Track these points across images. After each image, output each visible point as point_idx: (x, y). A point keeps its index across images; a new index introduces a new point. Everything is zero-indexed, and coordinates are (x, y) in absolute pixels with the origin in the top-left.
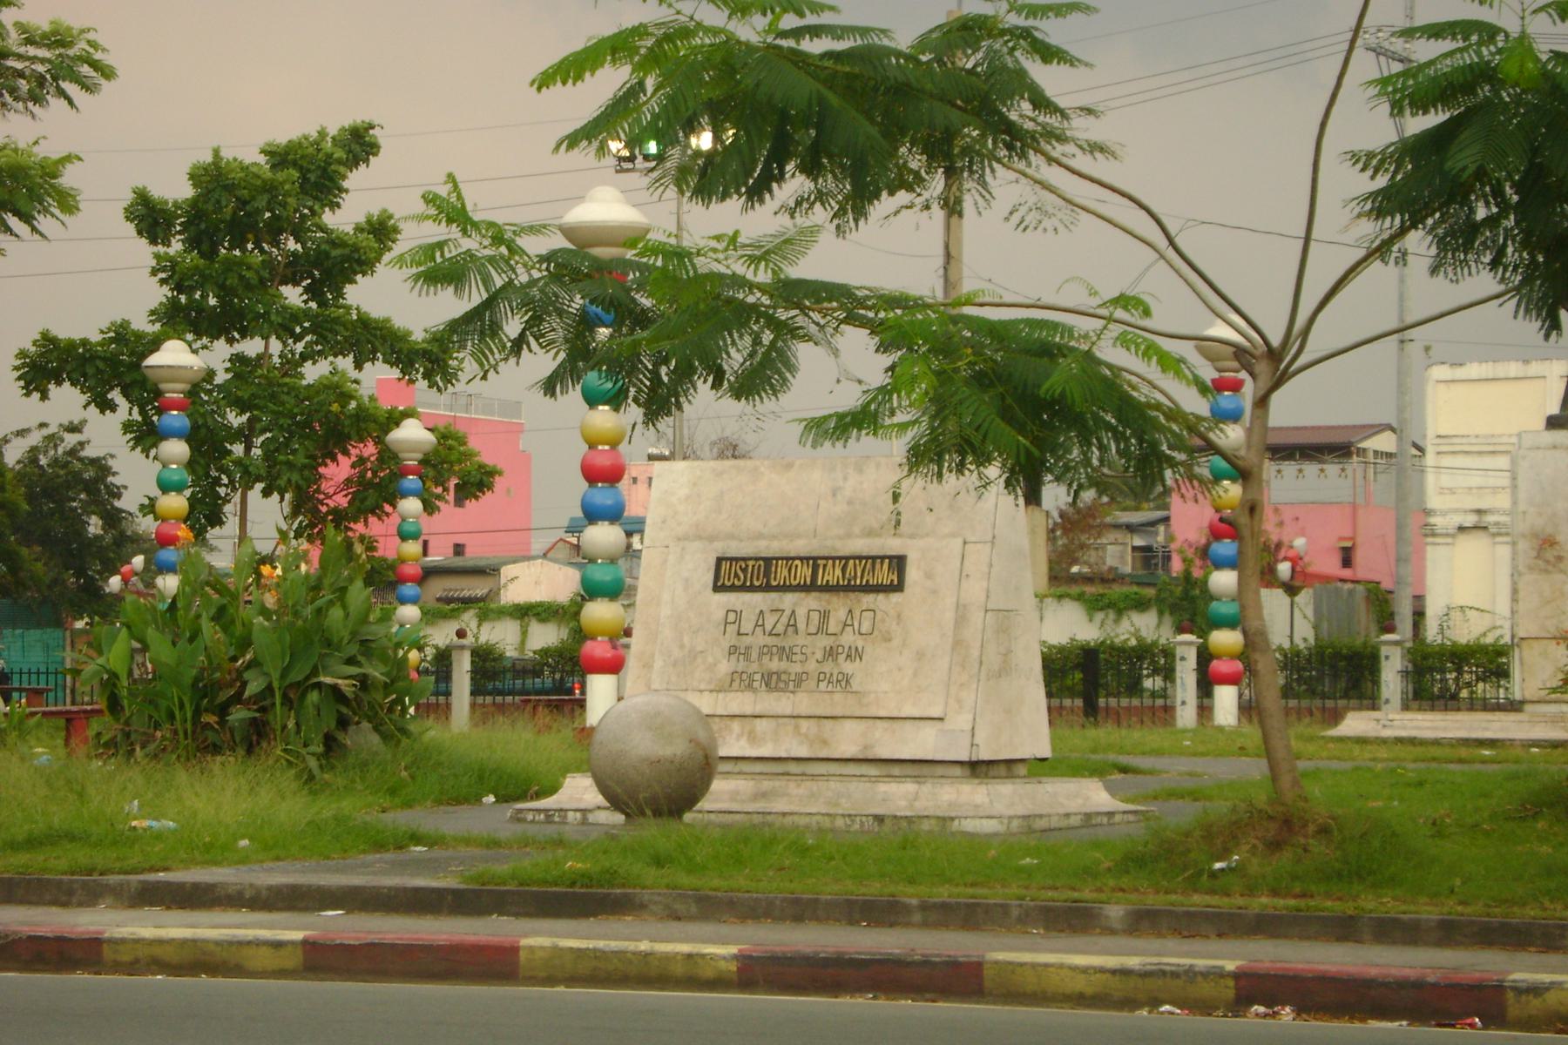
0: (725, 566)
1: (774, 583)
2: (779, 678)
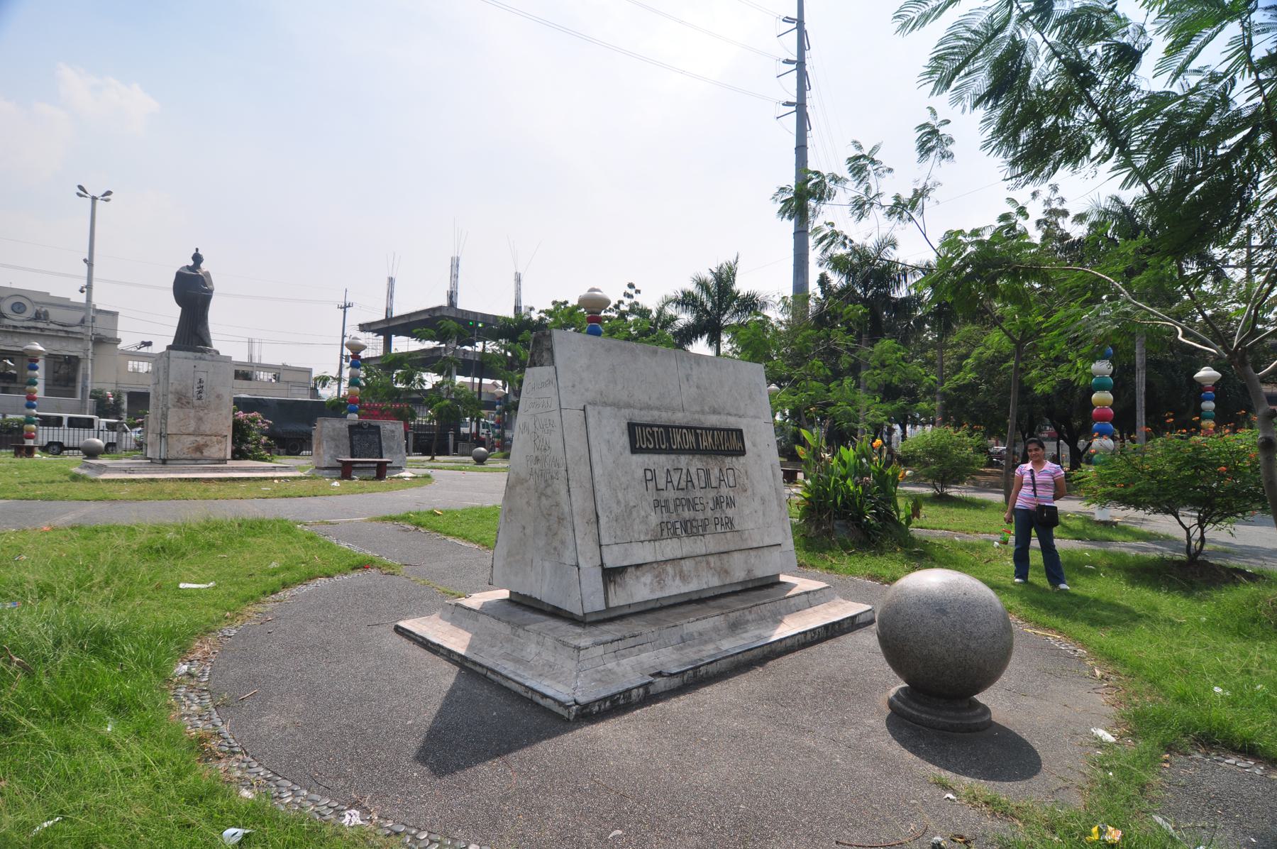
0: (638, 430)
1: (675, 447)
2: (691, 524)
